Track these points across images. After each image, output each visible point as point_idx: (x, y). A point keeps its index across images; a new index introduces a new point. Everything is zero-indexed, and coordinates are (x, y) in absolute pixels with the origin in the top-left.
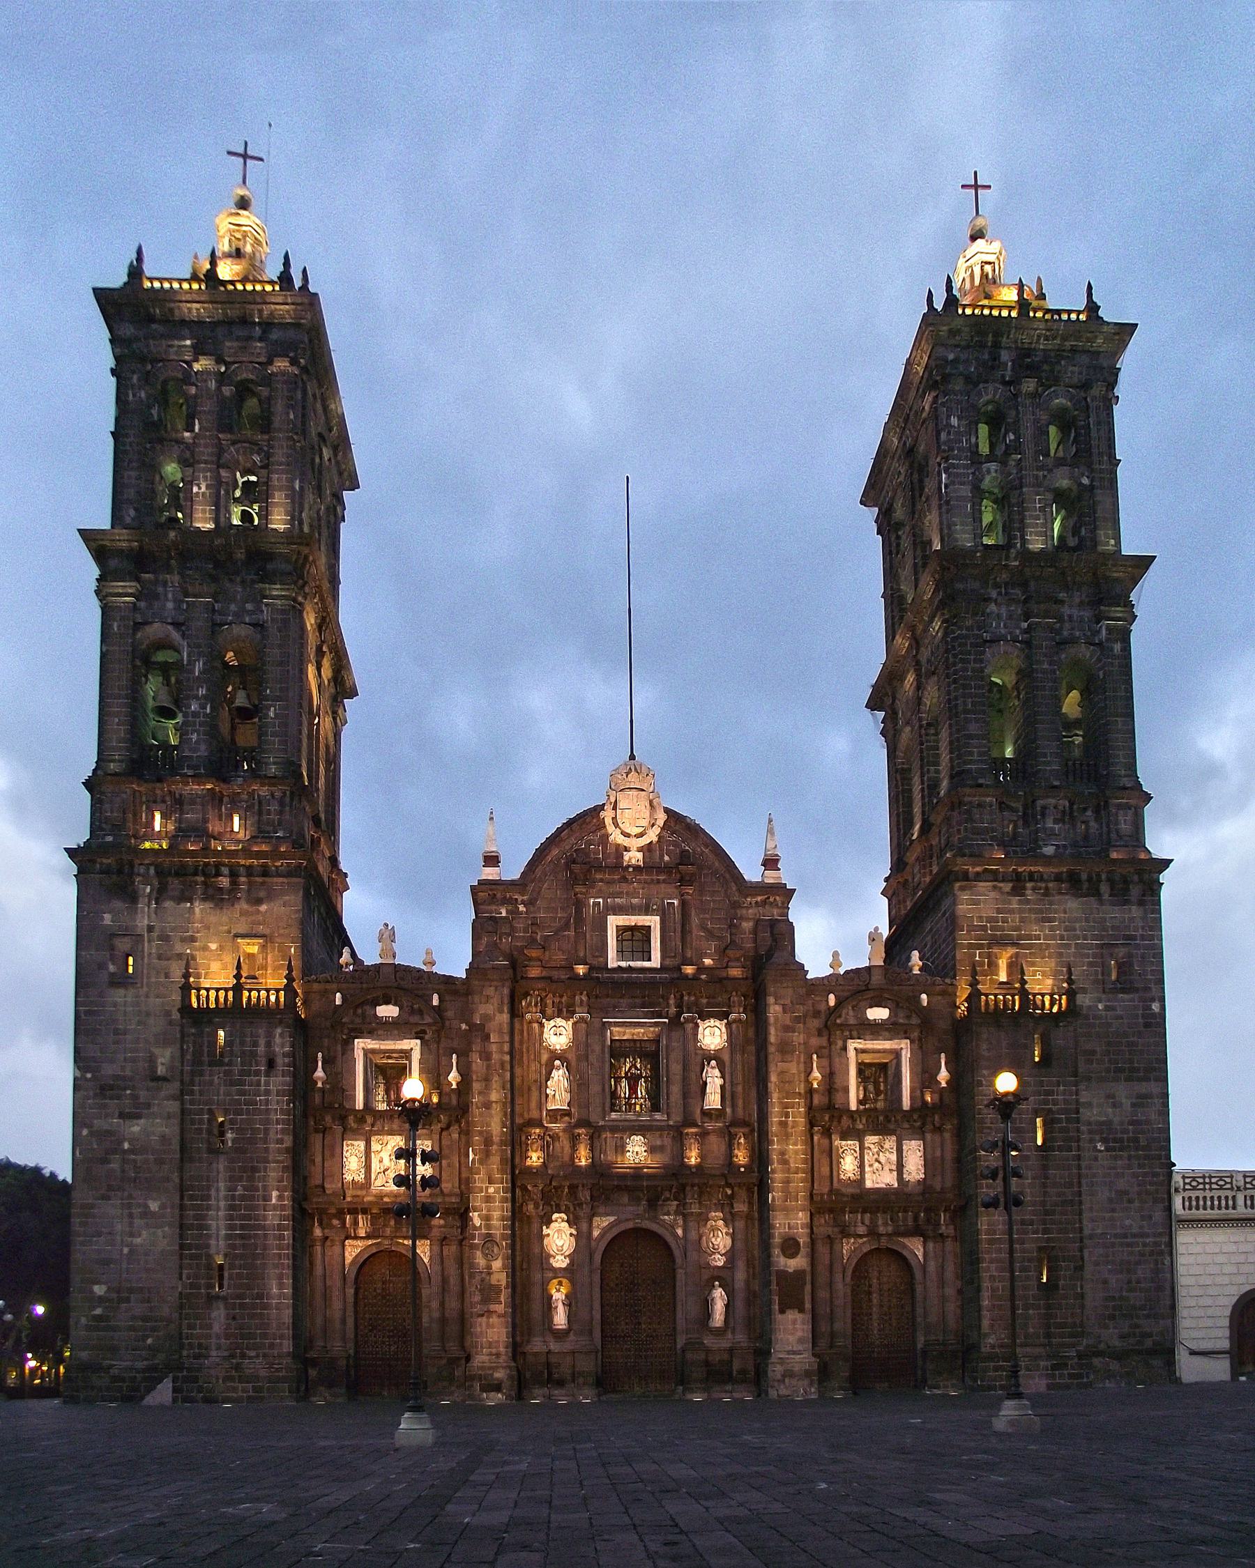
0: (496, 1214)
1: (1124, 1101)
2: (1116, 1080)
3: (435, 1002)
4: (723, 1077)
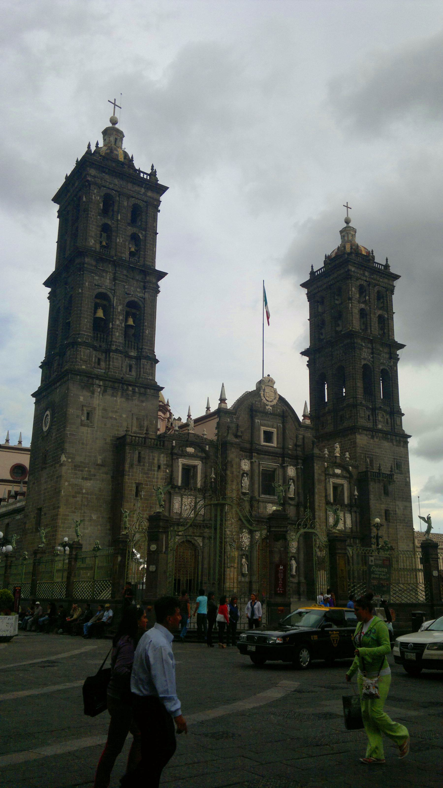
3: (207, 448)
4: (294, 486)
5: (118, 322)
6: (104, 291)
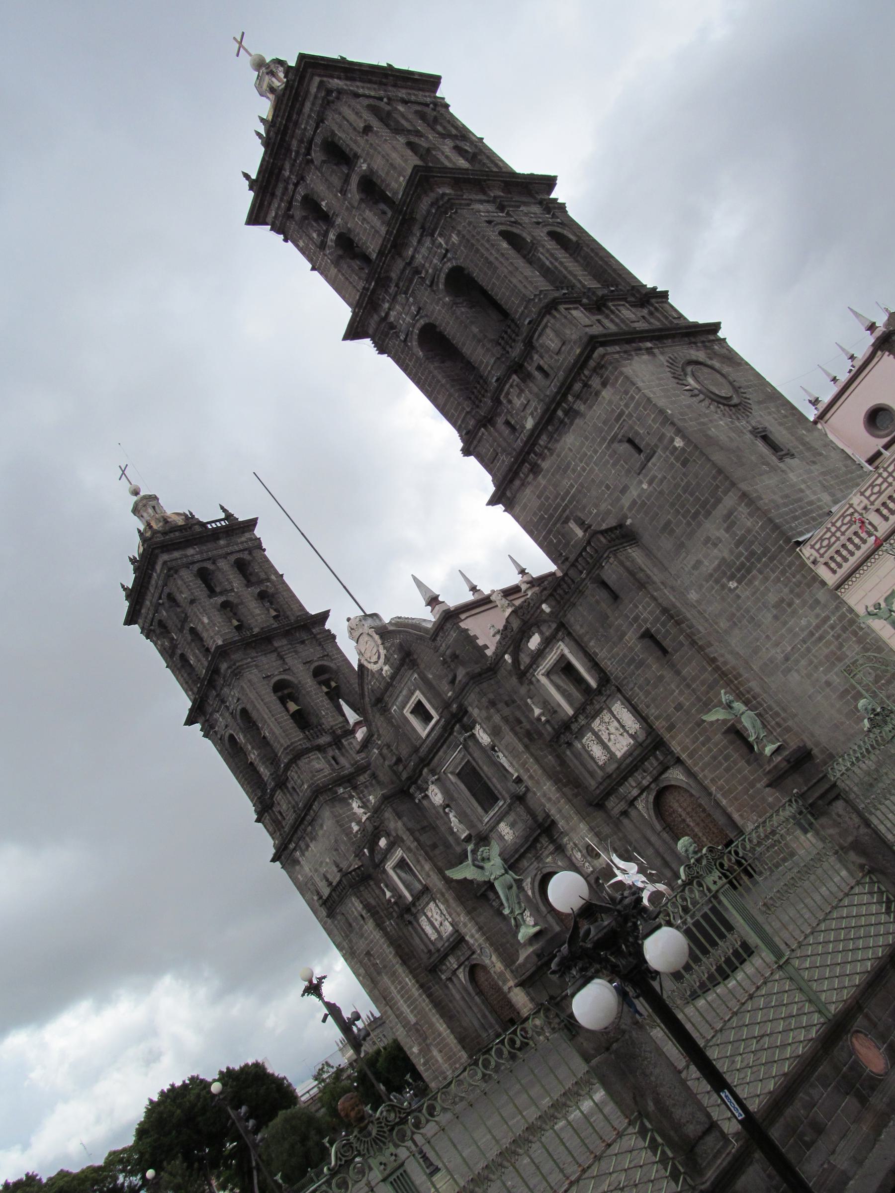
0: (473, 931)
1: (718, 534)
2: (699, 525)
5: (253, 756)
6: (227, 735)
